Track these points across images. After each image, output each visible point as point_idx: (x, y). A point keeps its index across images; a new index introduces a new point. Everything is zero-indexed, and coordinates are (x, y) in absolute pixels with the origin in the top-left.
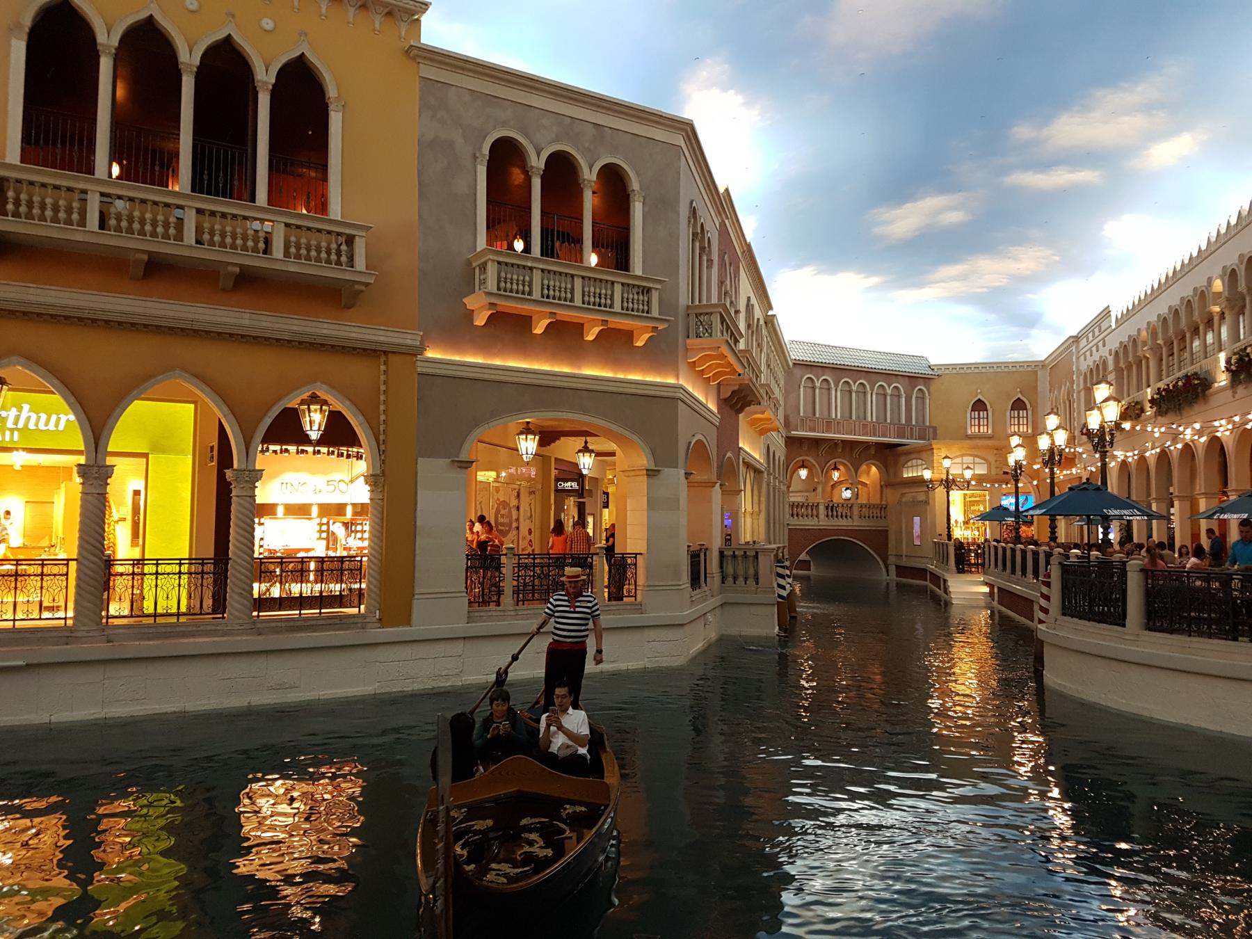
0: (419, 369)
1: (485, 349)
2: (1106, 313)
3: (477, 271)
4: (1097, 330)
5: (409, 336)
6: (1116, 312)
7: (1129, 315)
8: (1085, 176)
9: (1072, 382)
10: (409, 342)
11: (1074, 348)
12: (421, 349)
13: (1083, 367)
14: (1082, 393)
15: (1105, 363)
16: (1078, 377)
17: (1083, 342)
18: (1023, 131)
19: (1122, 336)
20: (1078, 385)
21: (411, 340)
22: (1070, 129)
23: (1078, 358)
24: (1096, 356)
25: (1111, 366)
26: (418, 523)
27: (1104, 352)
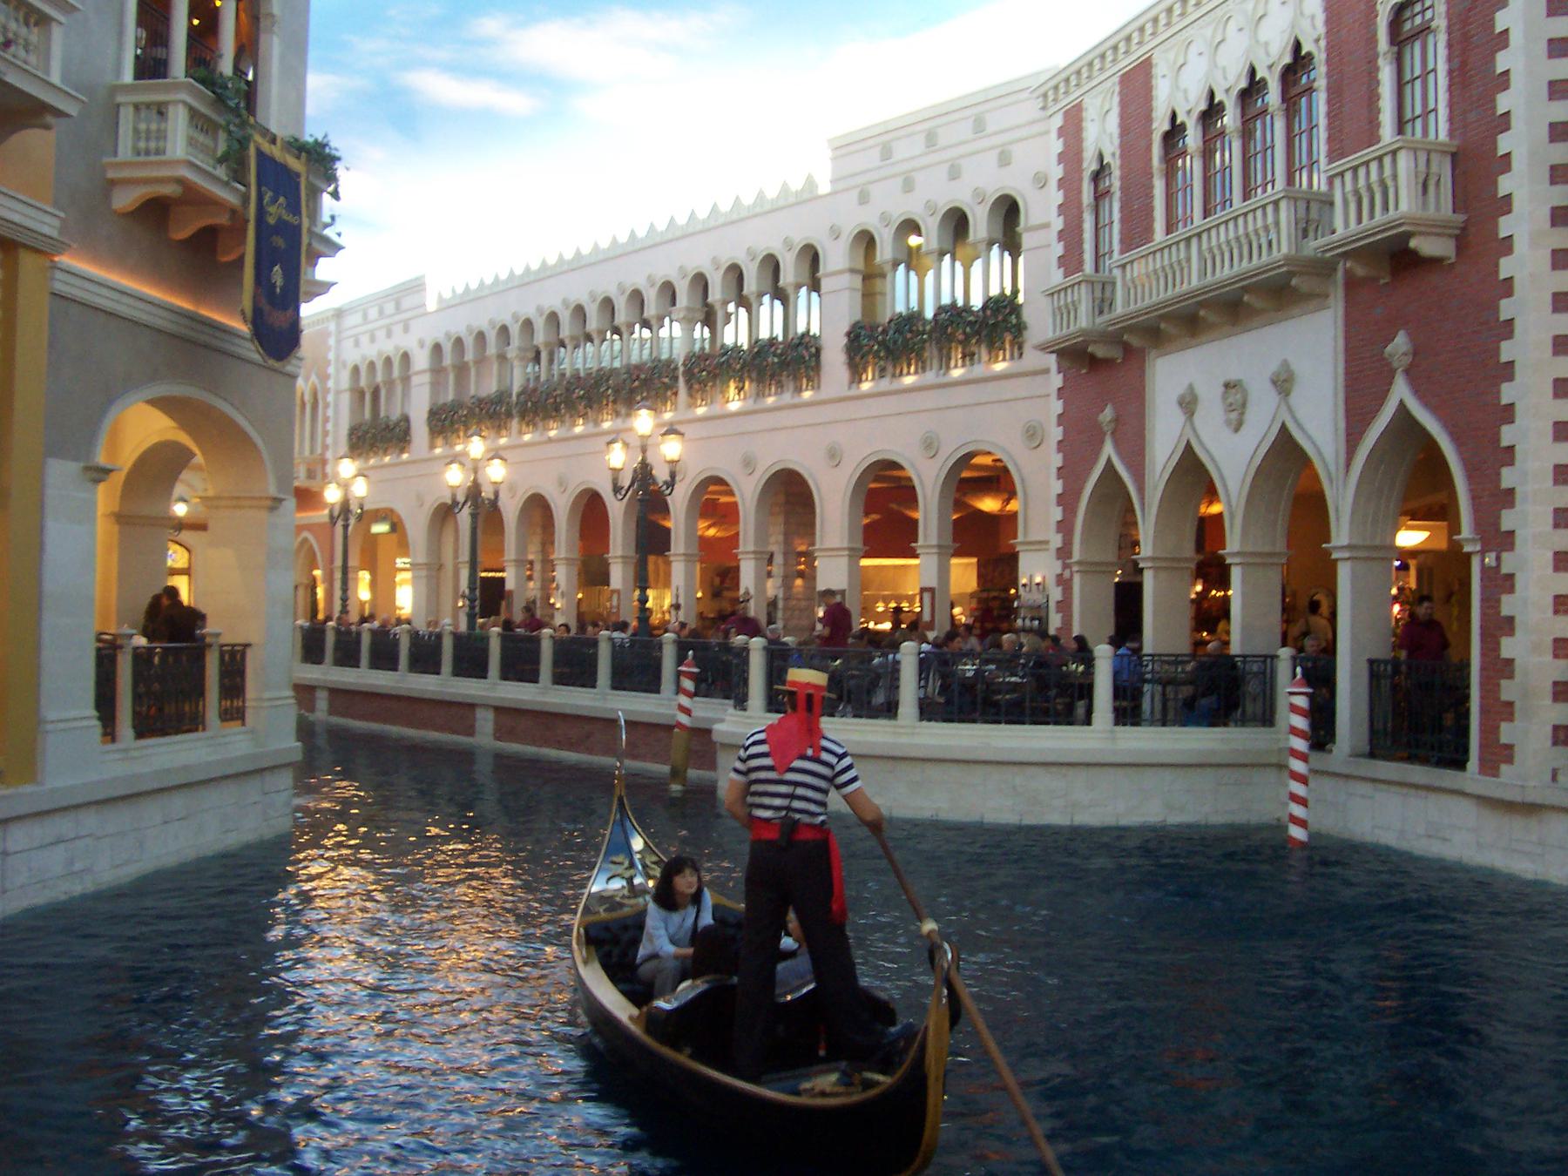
0: (59, 287)
1: (117, 260)
2: (415, 287)
3: (127, 115)
4: (390, 308)
5: (47, 219)
6: (441, 286)
7: (469, 298)
8: (513, 101)
9: (324, 377)
10: (46, 230)
11: (332, 327)
12: (62, 247)
13: (353, 356)
14: (346, 399)
15: (406, 357)
16: (337, 370)
17: (352, 320)
18: (490, 25)
19: (461, 324)
20: (337, 382)
21: (48, 226)
22: (547, 43)
23: (339, 342)
24: (388, 347)
25: (421, 360)
26: (49, 586)
27: (409, 342)
